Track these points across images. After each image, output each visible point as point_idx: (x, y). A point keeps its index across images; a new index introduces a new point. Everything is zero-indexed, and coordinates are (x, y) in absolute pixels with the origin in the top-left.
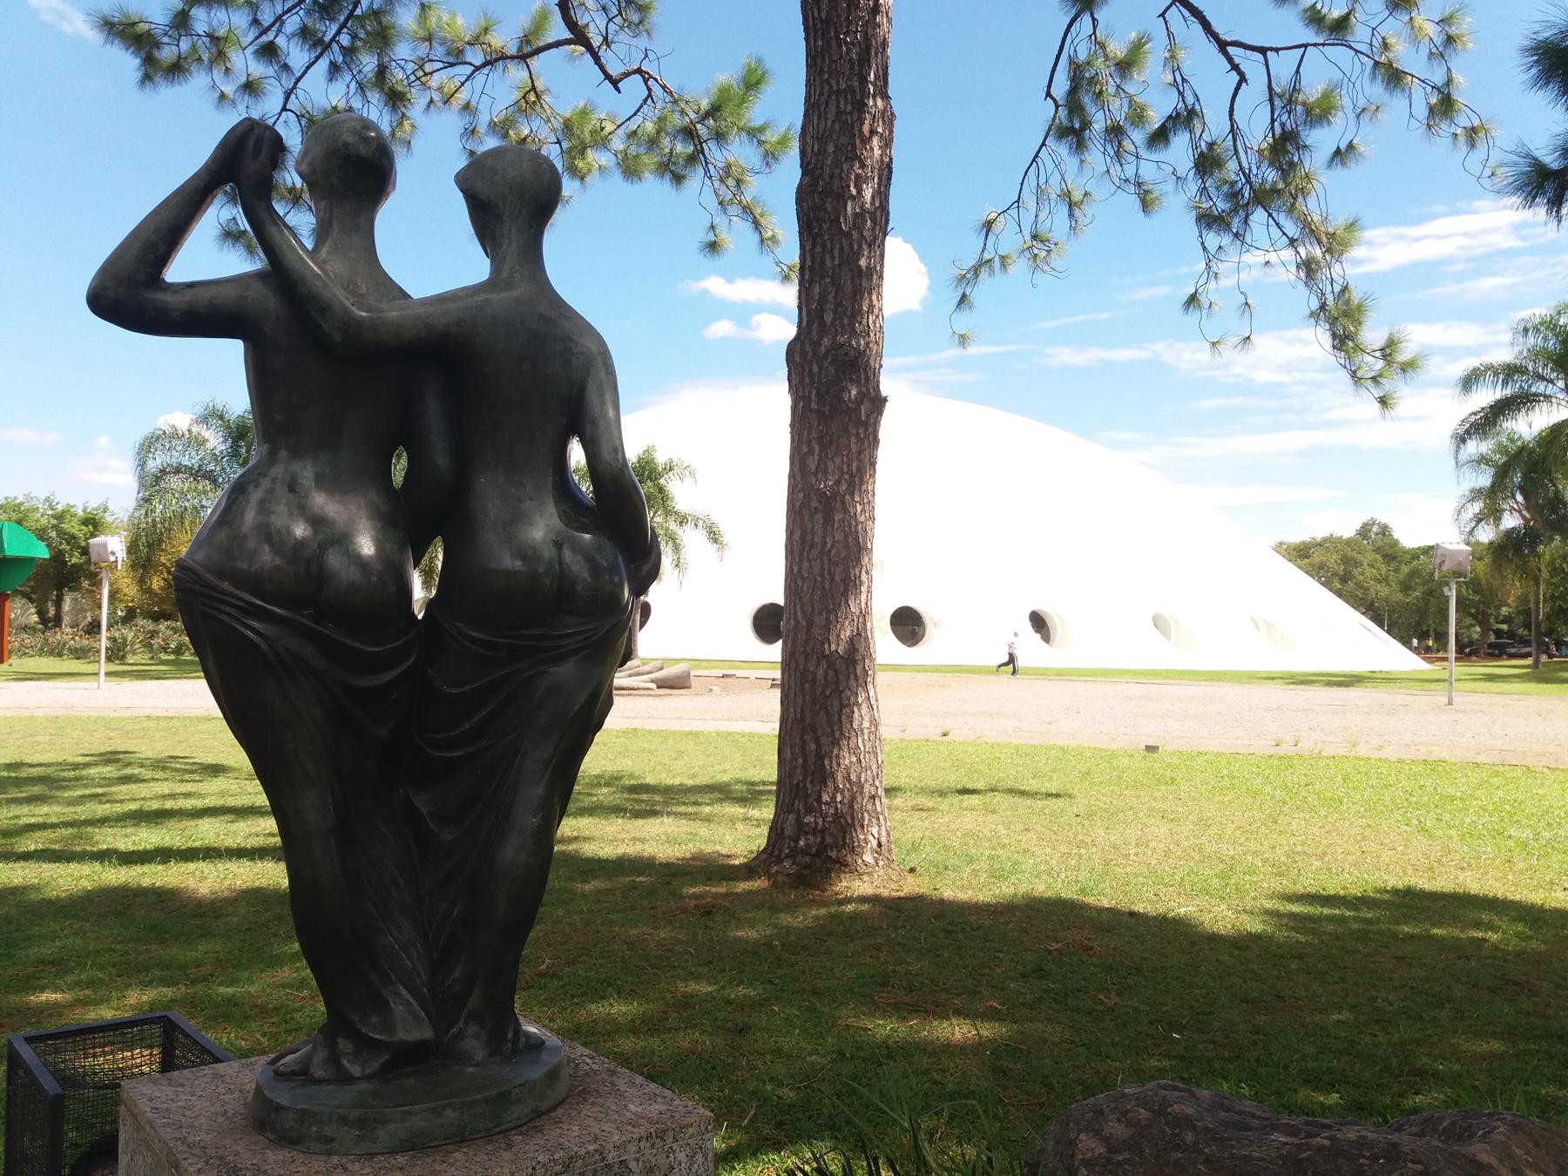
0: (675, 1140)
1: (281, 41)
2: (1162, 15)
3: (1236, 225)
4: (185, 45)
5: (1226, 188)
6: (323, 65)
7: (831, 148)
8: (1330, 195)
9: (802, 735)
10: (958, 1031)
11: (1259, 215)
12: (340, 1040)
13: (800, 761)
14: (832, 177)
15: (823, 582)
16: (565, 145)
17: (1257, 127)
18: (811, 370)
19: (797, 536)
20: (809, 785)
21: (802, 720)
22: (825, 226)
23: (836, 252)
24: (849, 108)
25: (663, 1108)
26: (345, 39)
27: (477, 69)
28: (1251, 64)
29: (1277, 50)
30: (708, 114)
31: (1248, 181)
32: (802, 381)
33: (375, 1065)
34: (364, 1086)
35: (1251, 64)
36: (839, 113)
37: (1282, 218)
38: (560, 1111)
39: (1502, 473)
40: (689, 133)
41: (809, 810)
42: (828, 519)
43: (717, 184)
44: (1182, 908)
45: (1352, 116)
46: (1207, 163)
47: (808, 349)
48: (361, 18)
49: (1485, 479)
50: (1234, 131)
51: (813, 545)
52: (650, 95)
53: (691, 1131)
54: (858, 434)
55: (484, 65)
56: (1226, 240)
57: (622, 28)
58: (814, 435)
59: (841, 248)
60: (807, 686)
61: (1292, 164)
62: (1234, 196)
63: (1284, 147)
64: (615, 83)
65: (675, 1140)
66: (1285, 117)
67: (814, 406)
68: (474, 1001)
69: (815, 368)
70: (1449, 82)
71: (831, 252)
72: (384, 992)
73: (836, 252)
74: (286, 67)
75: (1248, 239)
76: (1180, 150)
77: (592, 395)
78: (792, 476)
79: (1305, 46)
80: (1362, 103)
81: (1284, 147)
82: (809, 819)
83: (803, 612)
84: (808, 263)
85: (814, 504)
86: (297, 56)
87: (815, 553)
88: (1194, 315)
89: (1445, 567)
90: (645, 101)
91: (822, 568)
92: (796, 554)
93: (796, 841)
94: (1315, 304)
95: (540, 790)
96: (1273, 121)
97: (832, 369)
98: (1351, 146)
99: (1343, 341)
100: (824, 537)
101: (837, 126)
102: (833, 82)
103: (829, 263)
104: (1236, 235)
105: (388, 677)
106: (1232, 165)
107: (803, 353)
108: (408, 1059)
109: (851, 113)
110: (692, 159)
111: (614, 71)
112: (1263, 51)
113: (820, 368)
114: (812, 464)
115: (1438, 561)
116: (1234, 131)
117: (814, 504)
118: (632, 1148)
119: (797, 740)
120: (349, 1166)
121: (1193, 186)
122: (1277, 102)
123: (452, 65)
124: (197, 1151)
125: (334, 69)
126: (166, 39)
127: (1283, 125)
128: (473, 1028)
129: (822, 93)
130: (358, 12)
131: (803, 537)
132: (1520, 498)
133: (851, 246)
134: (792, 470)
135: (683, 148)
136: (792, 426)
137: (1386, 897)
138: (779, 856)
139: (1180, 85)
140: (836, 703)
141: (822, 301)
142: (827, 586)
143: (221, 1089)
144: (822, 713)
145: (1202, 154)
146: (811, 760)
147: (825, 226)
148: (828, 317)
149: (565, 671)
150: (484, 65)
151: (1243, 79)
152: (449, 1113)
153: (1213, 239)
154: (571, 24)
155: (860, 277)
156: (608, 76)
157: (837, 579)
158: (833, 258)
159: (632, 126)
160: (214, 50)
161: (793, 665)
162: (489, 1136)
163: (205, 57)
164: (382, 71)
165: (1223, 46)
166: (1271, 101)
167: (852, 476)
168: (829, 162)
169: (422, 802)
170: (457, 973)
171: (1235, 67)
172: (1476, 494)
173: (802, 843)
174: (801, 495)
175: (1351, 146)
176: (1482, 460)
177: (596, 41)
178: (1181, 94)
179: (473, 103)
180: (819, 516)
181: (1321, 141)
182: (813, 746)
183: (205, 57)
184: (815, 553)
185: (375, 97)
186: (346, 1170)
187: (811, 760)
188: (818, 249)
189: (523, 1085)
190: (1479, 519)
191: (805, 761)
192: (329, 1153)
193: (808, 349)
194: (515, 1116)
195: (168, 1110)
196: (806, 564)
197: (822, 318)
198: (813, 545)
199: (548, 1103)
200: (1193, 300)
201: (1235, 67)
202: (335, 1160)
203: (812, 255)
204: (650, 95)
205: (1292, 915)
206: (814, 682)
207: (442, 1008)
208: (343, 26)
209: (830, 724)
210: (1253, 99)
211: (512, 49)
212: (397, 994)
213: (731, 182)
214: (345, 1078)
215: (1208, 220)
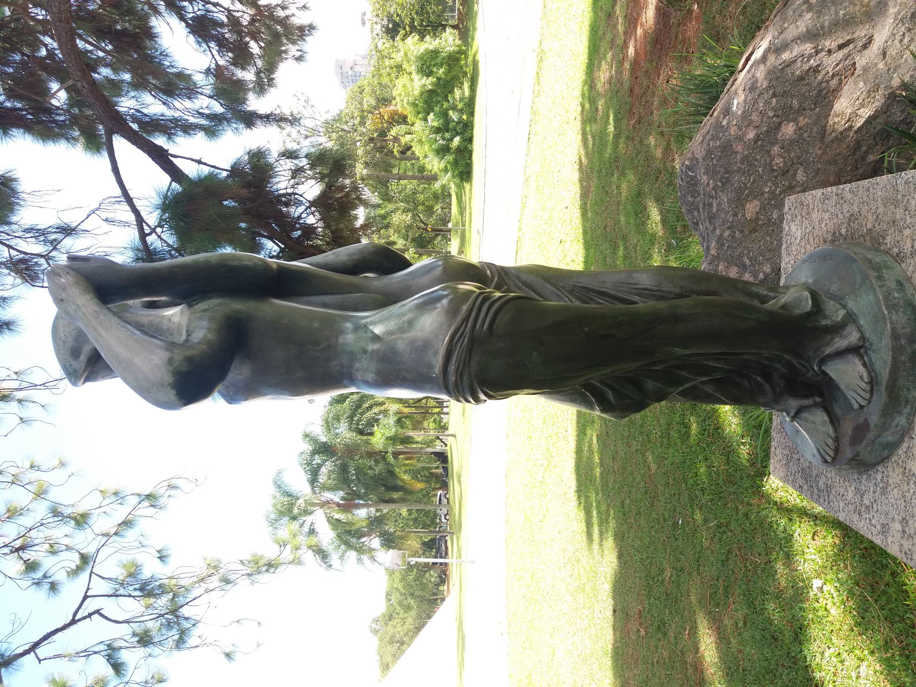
2: (40, 661)
3: (186, 625)
5: (164, 631)
8: (183, 566)
10: (708, 648)
11: (185, 611)
17: (131, 607)
28: (91, 605)
29: (88, 589)
31: (162, 615)
35: (91, 605)
37: (191, 596)
39: (349, 546)
44: (605, 588)
45: (143, 549)
46: (144, 640)
49: (352, 554)
50: (127, 622)
56: (195, 632)
61: (160, 586)
62: (169, 625)
63: (147, 590)
66: (131, 588)
70: (139, 495)
75: (197, 618)
76: (130, 657)
79: (92, 572)
80: (137, 544)
81: (147, 590)
88: (237, 656)
89: (400, 563)
94: (246, 581)
96: (130, 596)
98: (159, 552)
99: (271, 566)
104: (194, 625)
106: (150, 624)
112: (86, 597)
115: (396, 567)
116: (127, 622)
121: (155, 650)
122: (122, 592)
127: (135, 589)
132: (363, 540)
137: (583, 500)
139: (87, 653)
145: (138, 642)
151: (98, 612)
153: (192, 641)
165: (73, 622)
166: (117, 596)
171: (90, 615)
172: (359, 560)
175: (159, 552)
176: (341, 558)
178: (95, 653)
181: (151, 568)
190: (373, 559)
200: (228, 655)
201: (90, 615)
205: (601, 524)
210: (111, 607)
215: (180, 643)
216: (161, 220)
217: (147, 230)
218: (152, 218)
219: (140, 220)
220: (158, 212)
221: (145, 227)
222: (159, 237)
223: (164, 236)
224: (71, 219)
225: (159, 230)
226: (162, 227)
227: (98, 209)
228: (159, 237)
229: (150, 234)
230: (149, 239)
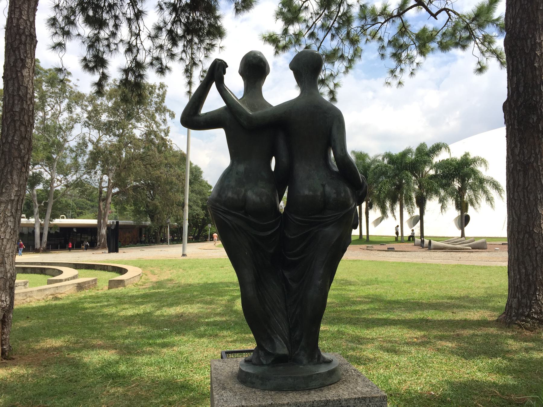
0: (370, 402)
1: (316, 31)
4: (287, 39)
6: (329, 36)
7: (518, 21)
9: (519, 265)
12: (260, 351)
13: (518, 277)
14: (519, 32)
15: (525, 201)
16: (417, 44)
18: (514, 113)
19: (511, 182)
20: (523, 287)
21: (518, 259)
22: (518, 53)
23: (523, 62)
25: (369, 390)
26: (336, 25)
27: (383, 24)
30: (474, 19)
32: (510, 117)
33: (270, 361)
34: (266, 367)
38: (333, 385)
40: (467, 28)
41: (523, 297)
42: (526, 172)
43: (480, 45)
47: (512, 104)
48: (340, 17)
51: (519, 185)
52: (450, 18)
53: (377, 399)
54: (538, 136)
55: (385, 22)
58: (517, 139)
59: (526, 60)
60: (519, 245)
64: (435, 16)
65: (370, 402)
67: (516, 127)
68: (303, 343)
69: (516, 111)
71: (521, 62)
72: (273, 337)
73: (523, 62)
74: (318, 39)
77: (335, 131)
78: (508, 157)
82: (524, 301)
83: (515, 213)
84: (511, 69)
85: (518, 168)
86: (321, 34)
87: (520, 189)
90: (448, 21)
91: (524, 195)
92: (512, 189)
93: (518, 310)
95: (321, 272)
97: (524, 111)
100: (524, 182)
101: (521, 11)
103: (520, 67)
105: (270, 233)
107: (510, 105)
108: (280, 360)
109: (527, 4)
110: (469, 38)
111: (434, 12)
113: (518, 111)
114: (517, 151)
117: (518, 168)
118: (352, 402)
119: (516, 268)
120: (257, 392)
123: (373, 25)
124: (218, 382)
125: (333, 36)
126: (281, 39)
128: (303, 352)
130: (340, 14)
131: (514, 182)
133: (530, 58)
134: (507, 155)
135: (466, 34)
136: (507, 137)
138: (511, 315)
140: (534, 252)
141: (518, 84)
142: (527, 202)
143: (235, 365)
144: (527, 257)
146: (523, 276)
147: (518, 53)
148: (521, 89)
149: (329, 230)
150: (385, 22)
152: (290, 379)
155: (536, 70)
156: (432, 14)
157: (531, 199)
158: (522, 65)
159: (444, 30)
160: (296, 40)
161: (513, 237)
162: (304, 390)
163: (293, 42)
164: (348, 33)
167: (536, 155)
168: (518, 26)
169: (286, 274)
170: (297, 333)
173: (521, 311)
174: (512, 165)
179: (382, 37)
180: (521, 173)
182: (524, 271)
183: (293, 42)
184: (520, 189)
185: (347, 43)
186: (255, 393)
187: (523, 276)
188: (515, 62)
189: (317, 374)
191: (520, 277)
192: (253, 387)
193: (512, 104)
194: (314, 385)
195: (218, 369)
196: (516, 194)
197: (518, 90)
198: (519, 185)
199: (328, 383)
202: (254, 390)
203: (512, 66)
204: (450, 18)
206: (523, 243)
207: (292, 344)
208: (335, 20)
209: (531, 261)
211: (395, 13)
212: (277, 338)
213: (486, 43)
214: (261, 364)
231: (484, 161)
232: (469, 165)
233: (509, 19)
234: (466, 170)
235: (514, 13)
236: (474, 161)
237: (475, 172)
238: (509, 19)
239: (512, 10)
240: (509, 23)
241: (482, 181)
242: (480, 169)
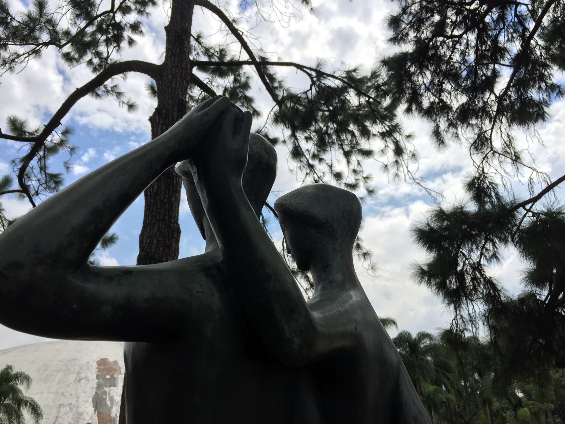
7: (155, 241)
24: (164, 227)
36: (159, 228)
57: (45, 189)
101: (158, 233)
102: (157, 216)
109: (164, 229)
129: (152, 220)
154: (21, 183)
168: (154, 246)
177: (32, 192)
216: (538, 214)
217: (528, 207)
218: (539, 207)
219: (534, 200)
220: (545, 210)
221: (530, 204)
222: (525, 215)
223: (526, 219)
224: (525, 158)
225: (530, 214)
226: (533, 216)
227: (537, 172)
228: (525, 215)
229: (525, 209)
230: (521, 209)
231: (27, 379)
232: (9, 382)
233: (145, 237)
234: (5, 387)
235: (151, 233)
236: (17, 376)
237: (15, 391)
238: (145, 237)
239: (150, 229)
240: (145, 241)
241: (20, 402)
242: (21, 387)
